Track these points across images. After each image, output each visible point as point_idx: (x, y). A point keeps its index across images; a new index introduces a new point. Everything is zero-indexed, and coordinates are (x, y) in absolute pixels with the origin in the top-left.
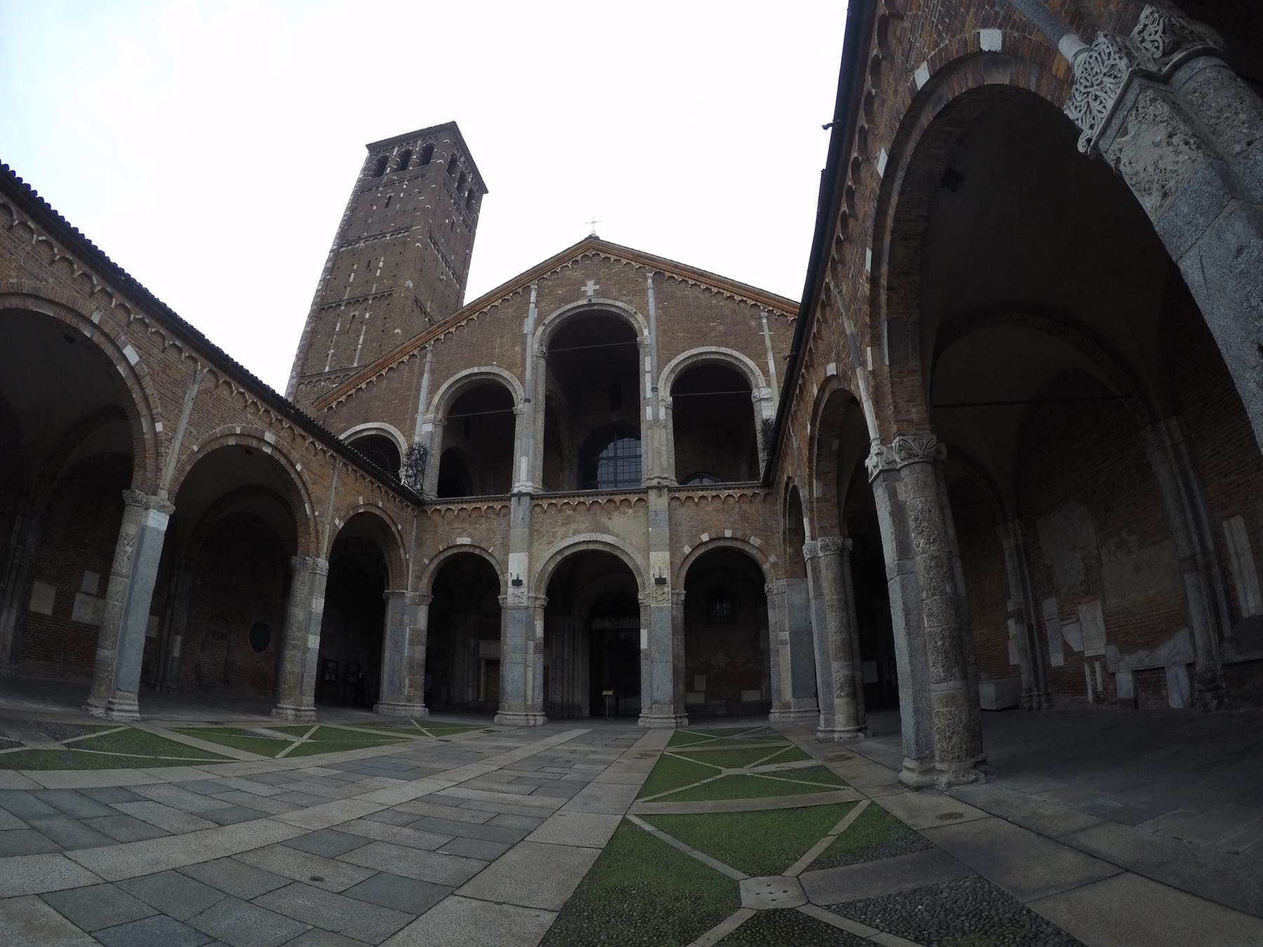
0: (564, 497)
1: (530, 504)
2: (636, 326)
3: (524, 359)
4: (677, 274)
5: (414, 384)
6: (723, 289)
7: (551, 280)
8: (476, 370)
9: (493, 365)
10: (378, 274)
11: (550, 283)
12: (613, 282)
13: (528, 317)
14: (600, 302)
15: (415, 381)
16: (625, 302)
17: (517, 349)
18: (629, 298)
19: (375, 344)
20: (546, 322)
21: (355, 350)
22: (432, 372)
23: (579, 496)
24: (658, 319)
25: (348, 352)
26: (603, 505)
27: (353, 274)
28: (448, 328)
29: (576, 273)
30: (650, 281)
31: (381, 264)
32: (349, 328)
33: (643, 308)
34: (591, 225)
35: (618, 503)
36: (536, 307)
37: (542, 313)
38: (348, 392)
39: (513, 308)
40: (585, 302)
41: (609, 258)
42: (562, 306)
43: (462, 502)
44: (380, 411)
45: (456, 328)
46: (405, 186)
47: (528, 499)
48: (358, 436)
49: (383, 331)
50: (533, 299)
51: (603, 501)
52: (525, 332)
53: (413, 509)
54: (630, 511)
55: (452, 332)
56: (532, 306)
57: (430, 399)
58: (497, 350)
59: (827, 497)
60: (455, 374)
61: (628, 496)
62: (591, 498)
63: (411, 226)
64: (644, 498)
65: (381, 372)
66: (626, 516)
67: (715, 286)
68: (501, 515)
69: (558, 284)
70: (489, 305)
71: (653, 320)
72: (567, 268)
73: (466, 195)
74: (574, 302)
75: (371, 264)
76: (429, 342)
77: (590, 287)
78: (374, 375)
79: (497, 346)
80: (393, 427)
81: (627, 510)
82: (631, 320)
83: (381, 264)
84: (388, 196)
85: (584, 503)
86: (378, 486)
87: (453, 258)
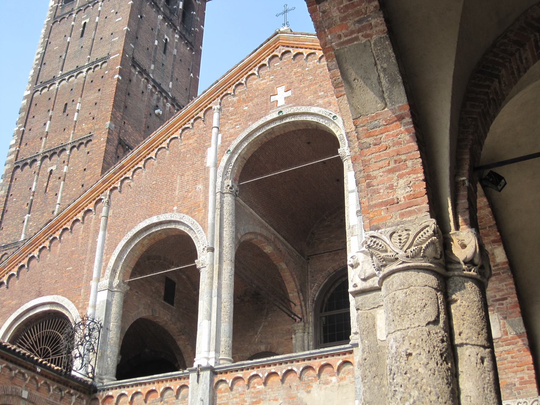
0: (253, 368)
1: (212, 381)
3: (206, 198)
8: (155, 219)
9: (172, 211)
10: (75, 119)
11: (235, 99)
12: (307, 83)
13: (210, 146)
14: (292, 111)
15: (90, 241)
17: (200, 187)
18: (327, 100)
20: (232, 148)
23: (269, 365)
25: (45, 214)
26: (299, 372)
28: (125, 173)
29: (263, 81)
32: (47, 187)
34: (282, 17)
35: (317, 369)
36: (219, 131)
37: (226, 138)
38: (20, 262)
40: (275, 115)
41: (301, 54)
42: (249, 125)
43: (137, 385)
44: (54, 281)
46: (100, 9)
47: (208, 373)
48: (32, 314)
50: (215, 123)
51: (298, 369)
52: (208, 165)
53: (79, 397)
54: (334, 379)
57: (108, 260)
58: (177, 192)
59: (510, 336)
60: (133, 227)
61: (330, 360)
62: (283, 365)
63: (109, 55)
64: (350, 360)
65: (55, 235)
66: (327, 386)
68: (180, 398)
69: (243, 99)
72: (253, 76)
73: (181, 7)
74: (261, 118)
75: (68, 108)
76: (105, 193)
79: (178, 187)
80: (66, 300)
81: (330, 378)
84: (83, 23)
85: (275, 373)
86: (20, 372)
87: (170, 86)
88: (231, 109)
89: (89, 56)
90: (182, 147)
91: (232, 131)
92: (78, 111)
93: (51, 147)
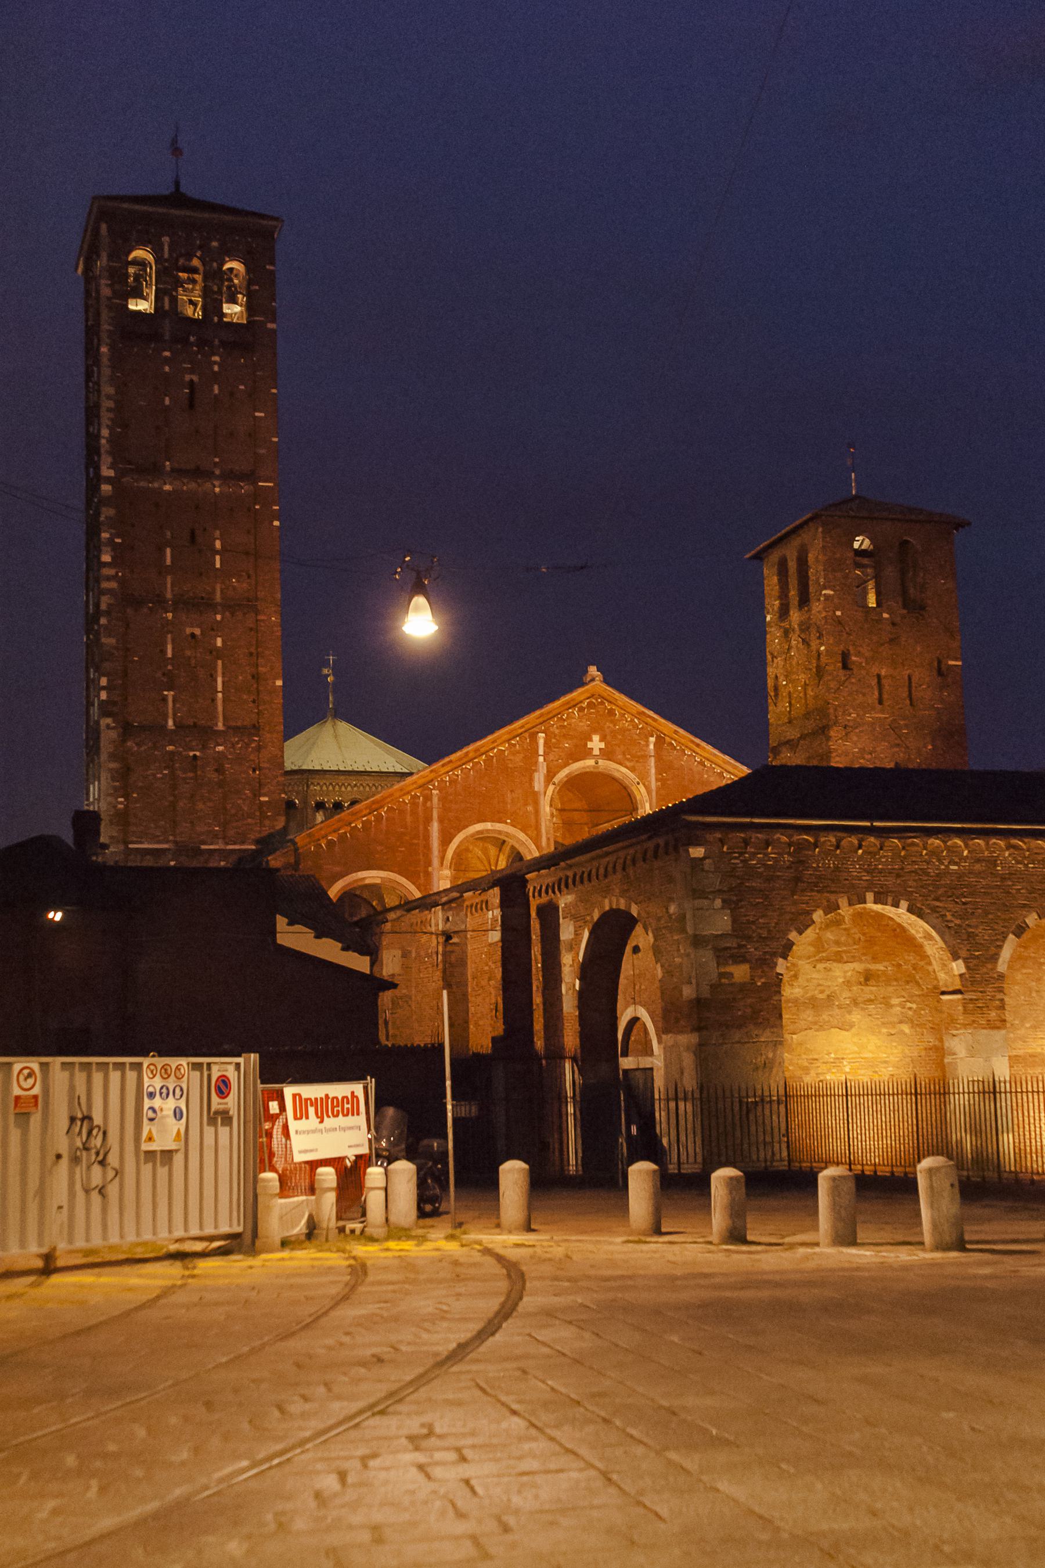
2: (638, 797)
4: (675, 740)
5: (421, 832)
6: (716, 764)
7: (557, 728)
9: (506, 823)
10: (218, 565)
13: (535, 771)
15: (421, 827)
16: (626, 767)
17: (530, 808)
19: (245, 697)
21: (214, 700)
22: (441, 821)
24: (657, 793)
27: (168, 551)
29: (581, 724)
30: (652, 747)
31: (218, 544)
33: (643, 778)
36: (545, 760)
39: (522, 755)
45: (462, 770)
46: (216, 368)
49: (253, 677)
50: (541, 752)
52: (536, 789)
55: (457, 776)
56: (541, 759)
67: (708, 760)
70: (494, 748)
71: (654, 794)
77: (596, 744)
78: (370, 813)
82: (634, 788)
83: (218, 544)
84: (187, 378)
88: (553, 740)
89: (217, 460)
90: (508, 762)
91: (555, 763)
92: (217, 552)
93: (182, 595)
